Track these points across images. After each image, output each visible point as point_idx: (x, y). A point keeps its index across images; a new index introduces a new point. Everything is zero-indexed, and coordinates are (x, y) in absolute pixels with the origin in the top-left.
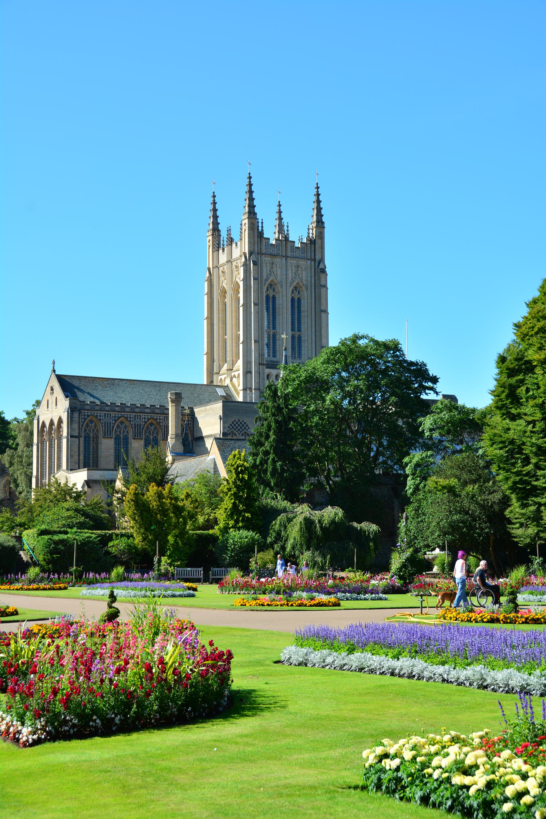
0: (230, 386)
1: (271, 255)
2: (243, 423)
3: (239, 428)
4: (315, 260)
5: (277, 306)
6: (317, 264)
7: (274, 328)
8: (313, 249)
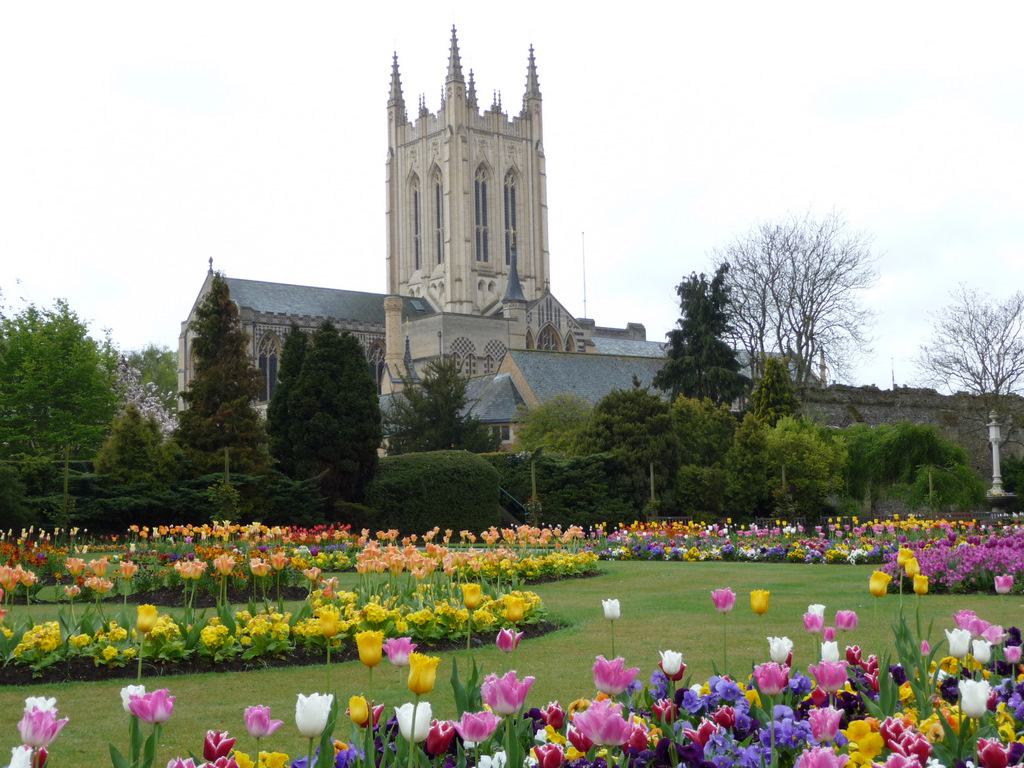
0: (429, 299)
1: (483, 132)
4: (532, 141)
5: (488, 197)
6: (534, 146)
7: (485, 224)
8: (529, 126)
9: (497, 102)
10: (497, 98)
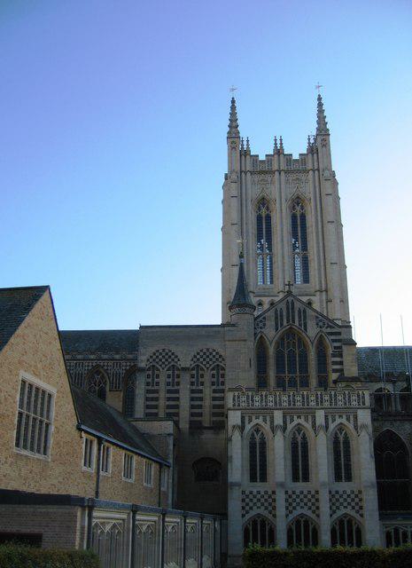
2: (170, 354)
3: (163, 360)
4: (319, 171)
9: (279, 146)
10: (278, 142)
